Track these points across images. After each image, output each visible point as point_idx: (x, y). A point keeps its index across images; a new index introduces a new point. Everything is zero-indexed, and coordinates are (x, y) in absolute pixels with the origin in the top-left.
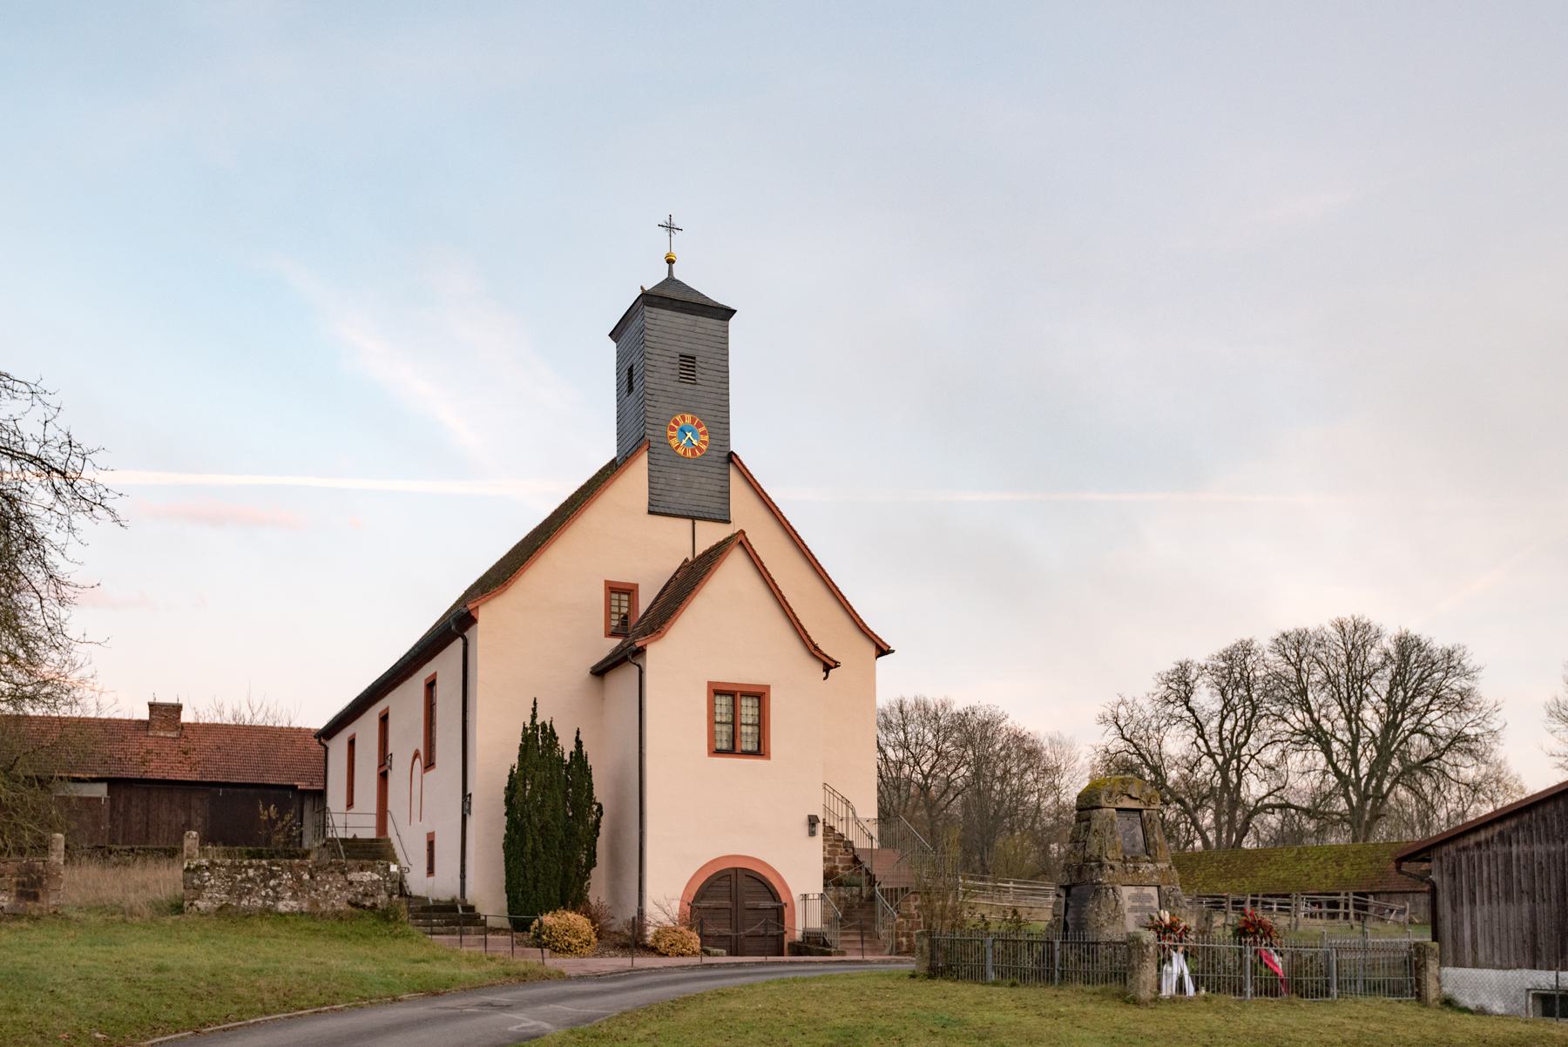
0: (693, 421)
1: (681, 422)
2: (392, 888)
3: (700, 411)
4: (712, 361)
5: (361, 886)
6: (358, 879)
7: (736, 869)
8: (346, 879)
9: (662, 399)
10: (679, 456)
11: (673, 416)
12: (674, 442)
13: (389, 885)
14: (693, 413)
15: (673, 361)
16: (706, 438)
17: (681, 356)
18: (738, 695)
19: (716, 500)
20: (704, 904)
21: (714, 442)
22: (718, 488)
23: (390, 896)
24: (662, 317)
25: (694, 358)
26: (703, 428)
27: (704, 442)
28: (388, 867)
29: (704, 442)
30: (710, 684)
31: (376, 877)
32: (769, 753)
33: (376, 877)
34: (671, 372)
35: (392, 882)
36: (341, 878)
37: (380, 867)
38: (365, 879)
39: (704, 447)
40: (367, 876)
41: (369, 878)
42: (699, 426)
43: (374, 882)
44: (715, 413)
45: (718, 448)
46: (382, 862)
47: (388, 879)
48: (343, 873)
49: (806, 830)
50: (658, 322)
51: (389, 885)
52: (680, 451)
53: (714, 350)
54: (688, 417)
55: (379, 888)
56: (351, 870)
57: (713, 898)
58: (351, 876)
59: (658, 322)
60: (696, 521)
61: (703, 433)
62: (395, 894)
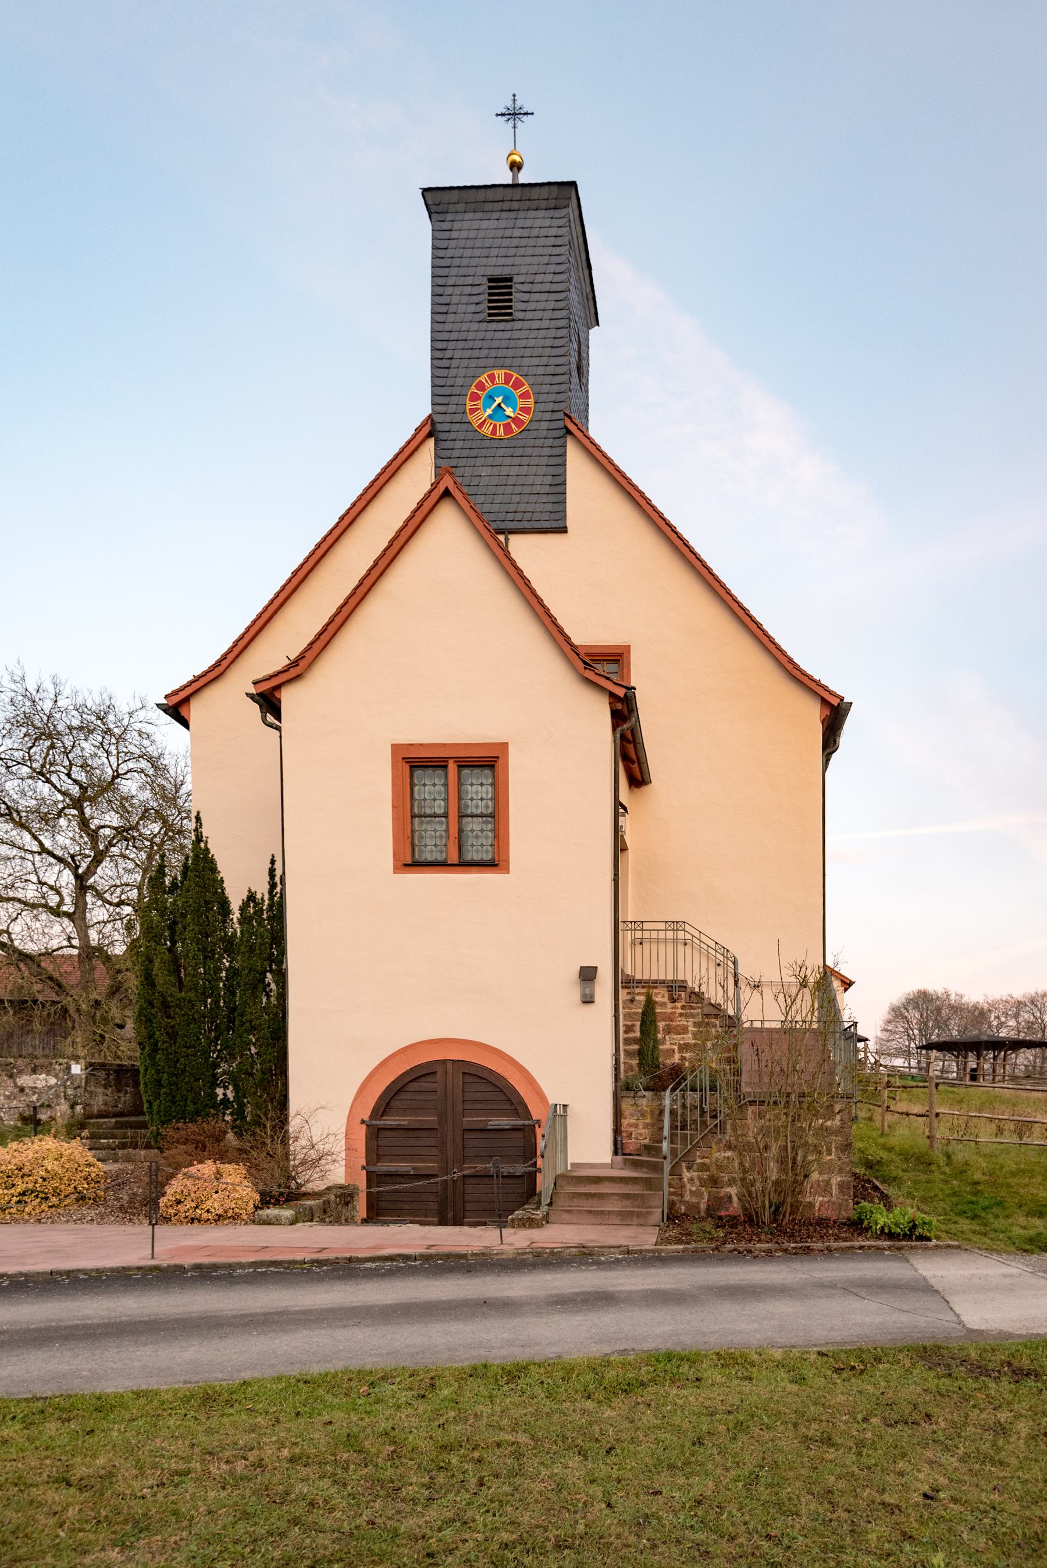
0: (508, 378)
1: (488, 385)
2: (75, 1096)
3: (517, 362)
4: (539, 278)
5: (34, 1093)
6: (31, 1084)
7: (444, 1061)
8: (16, 1085)
9: (458, 354)
10: (484, 438)
11: (475, 377)
12: (474, 419)
13: (70, 1092)
14: (502, 367)
15: (476, 290)
16: (530, 403)
17: (490, 280)
18: (452, 766)
19: (544, 499)
20: (390, 1121)
21: (541, 407)
22: (548, 480)
23: (72, 1107)
24: (466, 225)
25: (510, 280)
26: (526, 388)
27: (525, 410)
28: (69, 1068)
29: (525, 410)
30: (396, 748)
31: (53, 1081)
32: (507, 861)
33: (53, 1081)
34: (473, 308)
35: (75, 1089)
36: (10, 1082)
37: (57, 1067)
38: (40, 1084)
39: (526, 418)
40: (42, 1080)
41: (44, 1083)
42: (517, 385)
43: (50, 1088)
44: (544, 361)
45: (548, 416)
46: (60, 1060)
47: (69, 1083)
48: (11, 1076)
49: (575, 994)
50: (454, 235)
51: (70, 1092)
52: (487, 430)
53: (546, 259)
54: (500, 374)
55: (58, 1096)
56: (21, 1072)
57: (405, 1111)
58: (25, 1080)
59: (454, 235)
60: (511, 537)
61: (525, 396)
62: (78, 1104)
